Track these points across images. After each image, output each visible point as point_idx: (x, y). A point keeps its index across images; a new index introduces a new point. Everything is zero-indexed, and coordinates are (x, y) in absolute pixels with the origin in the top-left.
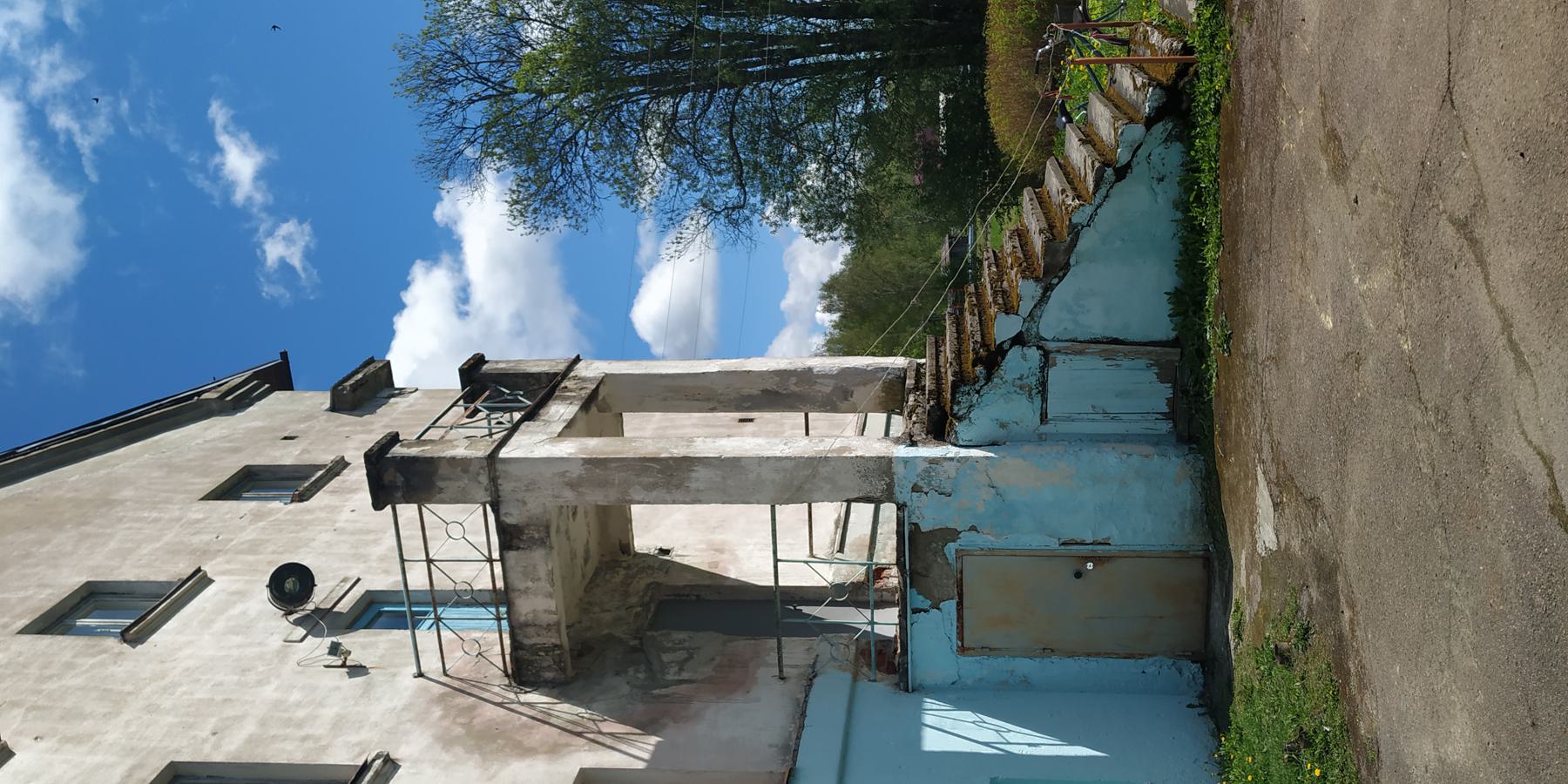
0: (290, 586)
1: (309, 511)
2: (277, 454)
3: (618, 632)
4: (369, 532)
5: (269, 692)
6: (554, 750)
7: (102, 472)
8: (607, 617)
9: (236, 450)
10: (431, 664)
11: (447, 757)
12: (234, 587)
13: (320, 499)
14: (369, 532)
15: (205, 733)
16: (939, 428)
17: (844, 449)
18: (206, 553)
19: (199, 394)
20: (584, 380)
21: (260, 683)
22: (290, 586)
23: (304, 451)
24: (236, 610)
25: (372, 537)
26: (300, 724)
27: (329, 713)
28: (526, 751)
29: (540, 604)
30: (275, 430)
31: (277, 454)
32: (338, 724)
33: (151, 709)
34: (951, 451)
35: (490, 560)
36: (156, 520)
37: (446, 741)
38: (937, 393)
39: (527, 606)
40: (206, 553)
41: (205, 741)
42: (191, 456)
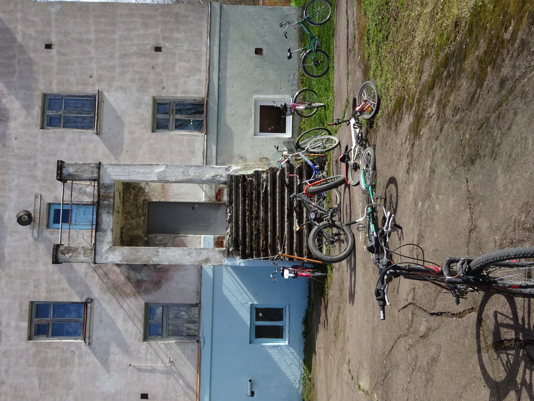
0: (25, 220)
3: (139, 232)
4: (29, 158)
8: (134, 222)
14: (29, 158)
15: (32, 288)
21: (37, 261)
25: (32, 162)
35: (92, 225)
41: (34, 292)
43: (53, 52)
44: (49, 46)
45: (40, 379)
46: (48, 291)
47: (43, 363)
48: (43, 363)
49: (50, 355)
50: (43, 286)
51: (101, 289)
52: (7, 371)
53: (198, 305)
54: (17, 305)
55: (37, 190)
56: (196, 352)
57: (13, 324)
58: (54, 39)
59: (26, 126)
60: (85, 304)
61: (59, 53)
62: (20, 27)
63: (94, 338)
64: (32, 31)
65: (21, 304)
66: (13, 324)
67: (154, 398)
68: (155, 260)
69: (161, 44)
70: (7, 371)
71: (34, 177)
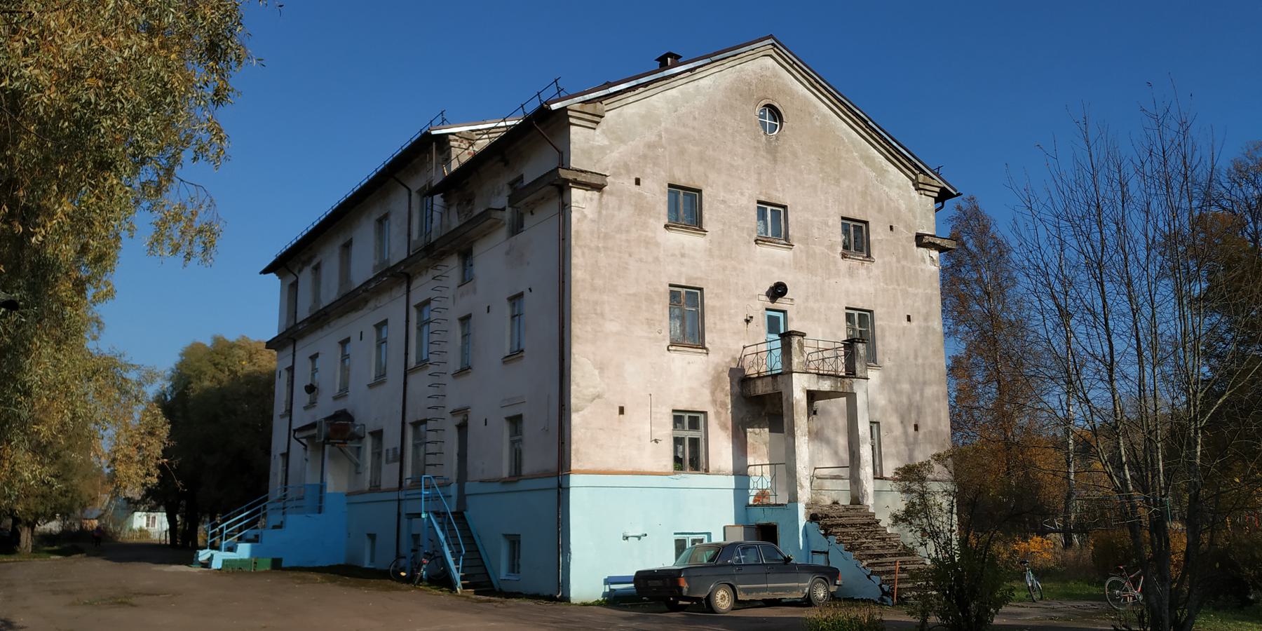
0: (778, 291)
1: (835, 263)
2: (879, 230)
5: (734, 301)
6: (714, 402)
7: (861, 163)
9: (880, 210)
10: (749, 351)
11: (710, 369)
12: (787, 262)
13: (844, 264)
16: (813, 518)
17: (802, 487)
18: (806, 240)
19: (922, 171)
20: (851, 386)
21: (738, 297)
22: (778, 291)
23: (880, 241)
24: (774, 269)
26: (721, 319)
27: (727, 325)
28: (713, 393)
29: (761, 388)
30: (898, 219)
31: (879, 230)
32: (723, 331)
33: (724, 269)
34: (802, 520)
36: (827, 207)
37: (715, 369)
38: (827, 516)
39: (759, 382)
40: (806, 240)
42: (875, 194)
43: (905, 322)
44: (909, 318)
45: (635, 295)
46: (713, 307)
47: (649, 299)
48: (649, 299)
49: (656, 306)
50: (717, 303)
51: (718, 364)
52: (641, 260)
53: (707, 471)
54: (699, 275)
55: (797, 301)
56: (664, 470)
57: (684, 269)
58: (914, 323)
59: (847, 293)
60: (704, 348)
61: (904, 328)
62: (921, 291)
63: (674, 355)
64: (918, 304)
65: (701, 279)
66: (684, 269)
67: (620, 421)
68: (798, 433)
69: (921, 431)
70: (641, 260)
71: (807, 299)
